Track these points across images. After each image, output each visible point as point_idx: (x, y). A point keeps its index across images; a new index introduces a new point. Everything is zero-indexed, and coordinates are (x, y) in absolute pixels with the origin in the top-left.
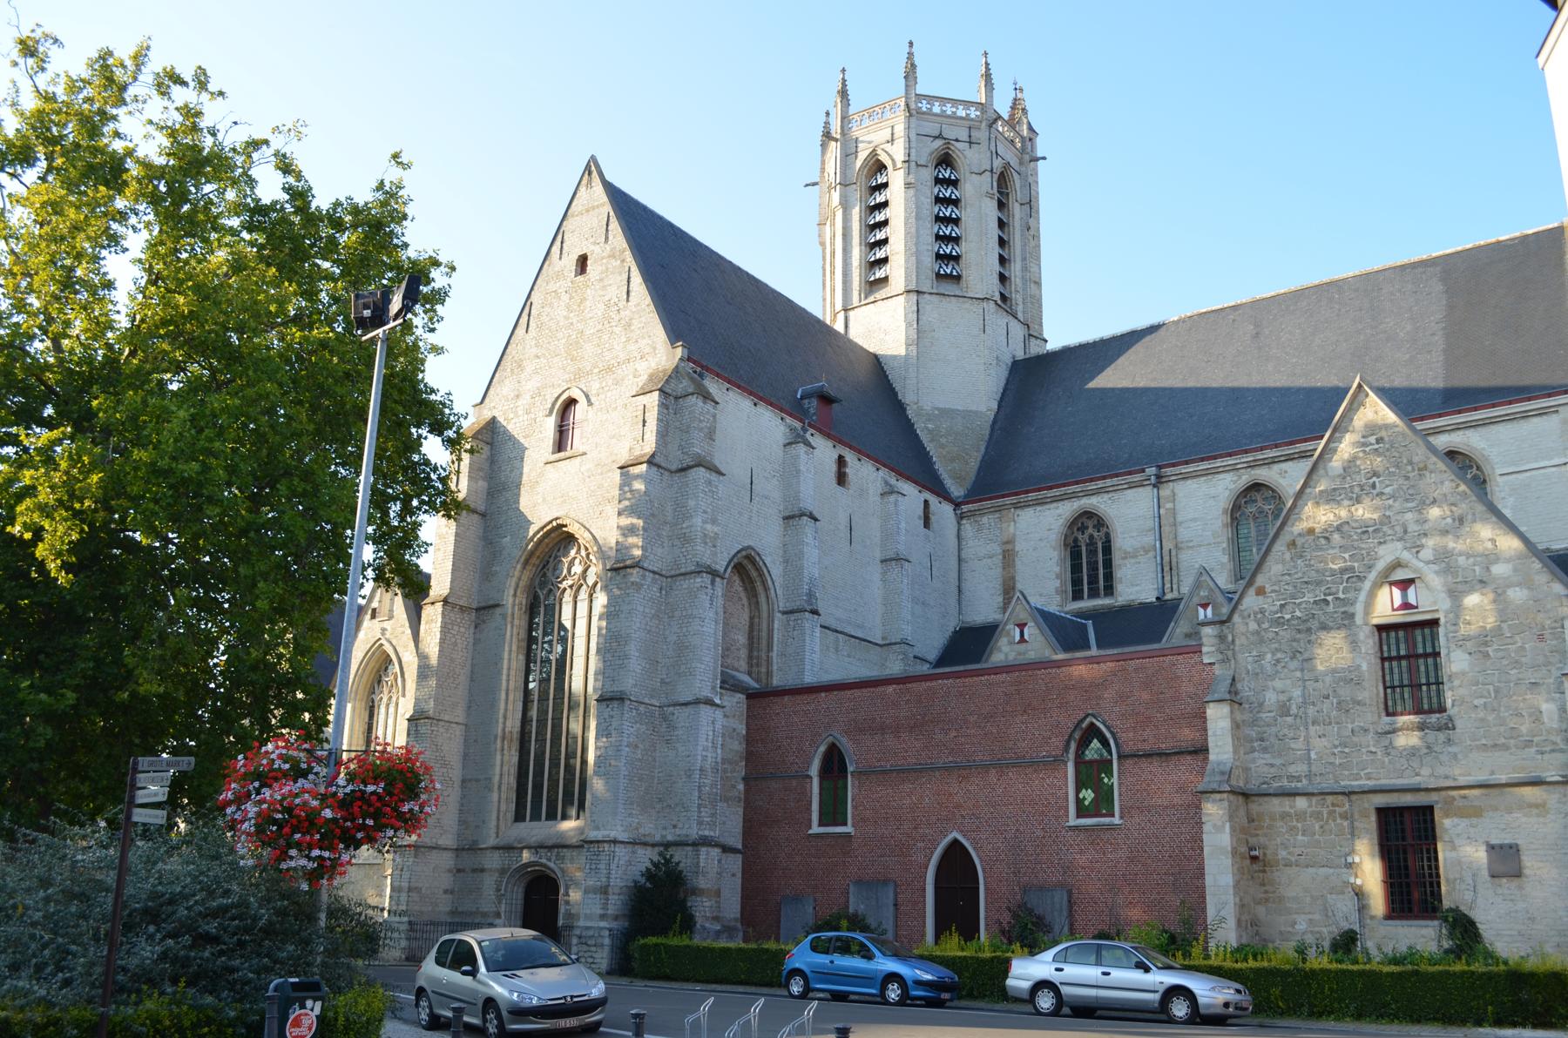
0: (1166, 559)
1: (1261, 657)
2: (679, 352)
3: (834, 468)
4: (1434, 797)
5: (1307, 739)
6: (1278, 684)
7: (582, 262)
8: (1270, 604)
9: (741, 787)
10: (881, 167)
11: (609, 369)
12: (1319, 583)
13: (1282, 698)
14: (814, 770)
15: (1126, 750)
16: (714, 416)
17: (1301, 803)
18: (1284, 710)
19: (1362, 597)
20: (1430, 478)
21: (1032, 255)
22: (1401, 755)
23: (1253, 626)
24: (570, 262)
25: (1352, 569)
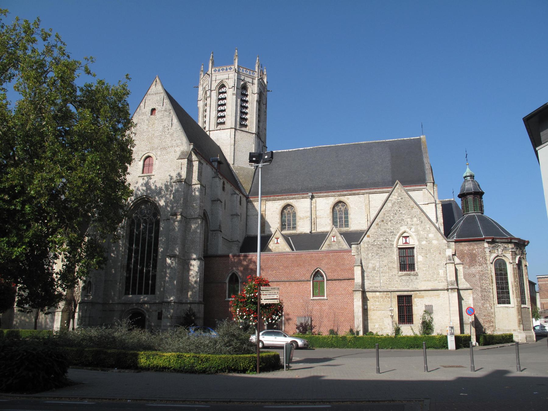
0: (313, 221)
1: (368, 254)
2: (192, 147)
4: (412, 293)
5: (380, 276)
6: (372, 262)
7: (153, 110)
8: (371, 240)
10: (223, 86)
11: (165, 148)
12: (384, 235)
13: (374, 265)
17: (378, 294)
18: (374, 269)
19: (396, 240)
20: (414, 210)
21: (265, 121)
22: (402, 283)
23: (366, 246)
24: (148, 110)
25: (393, 232)
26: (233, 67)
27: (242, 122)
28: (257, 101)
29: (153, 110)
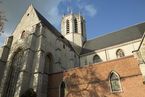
2: (40, 21)
3: (63, 46)
7: (28, 15)
9: (47, 91)
14: (60, 87)
15: (121, 77)
16: (45, 30)
26: (71, 14)
27: (76, 31)
28: (81, 24)
29: (28, 15)
